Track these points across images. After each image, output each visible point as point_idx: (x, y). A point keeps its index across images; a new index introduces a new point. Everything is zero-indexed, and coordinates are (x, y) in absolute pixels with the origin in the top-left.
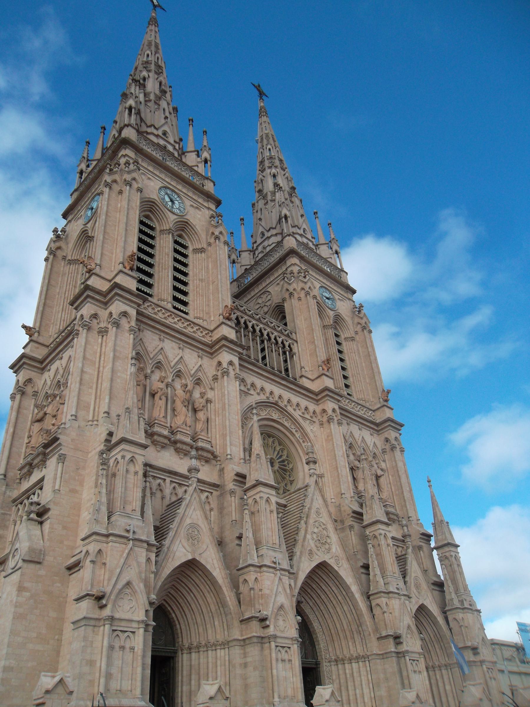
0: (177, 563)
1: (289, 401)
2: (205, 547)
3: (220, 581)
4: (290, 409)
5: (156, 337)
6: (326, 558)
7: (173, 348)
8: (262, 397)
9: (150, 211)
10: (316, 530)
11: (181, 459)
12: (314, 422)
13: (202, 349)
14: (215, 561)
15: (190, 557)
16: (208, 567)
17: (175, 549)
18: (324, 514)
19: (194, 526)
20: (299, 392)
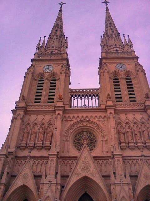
1: (91, 117)
2: (28, 180)
3: (33, 190)
4: (91, 119)
5: (35, 116)
6: (87, 175)
7: (41, 117)
8: (78, 119)
9: (41, 76)
10: (83, 165)
11: (39, 151)
12: (105, 120)
13: (52, 113)
14: (32, 184)
15: (22, 184)
16: (29, 186)
17: (17, 183)
18: (88, 158)
19: (25, 174)
20: (90, 112)
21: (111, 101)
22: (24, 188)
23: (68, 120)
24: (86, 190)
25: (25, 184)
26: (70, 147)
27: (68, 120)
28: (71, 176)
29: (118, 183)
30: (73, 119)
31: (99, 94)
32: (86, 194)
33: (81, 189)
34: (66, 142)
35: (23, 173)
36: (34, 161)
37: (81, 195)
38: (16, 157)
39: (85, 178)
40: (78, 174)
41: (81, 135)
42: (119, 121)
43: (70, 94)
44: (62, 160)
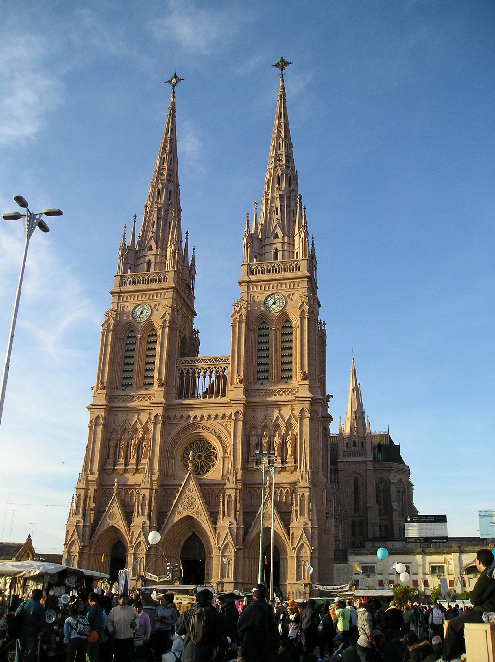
0: (105, 528)
6: (190, 513)
21: (242, 387)
22: (114, 529)
23: (174, 422)
24: (194, 530)
25: (114, 525)
26: (177, 468)
27: (174, 422)
28: (170, 516)
29: (225, 526)
30: (181, 422)
31: (227, 367)
32: (194, 534)
33: (187, 529)
34: (171, 460)
35: (111, 511)
36: (126, 490)
37: (188, 536)
38: (102, 485)
39: (189, 517)
40: (179, 512)
41: (194, 447)
42: (254, 422)
43: (179, 369)
44: (164, 489)
